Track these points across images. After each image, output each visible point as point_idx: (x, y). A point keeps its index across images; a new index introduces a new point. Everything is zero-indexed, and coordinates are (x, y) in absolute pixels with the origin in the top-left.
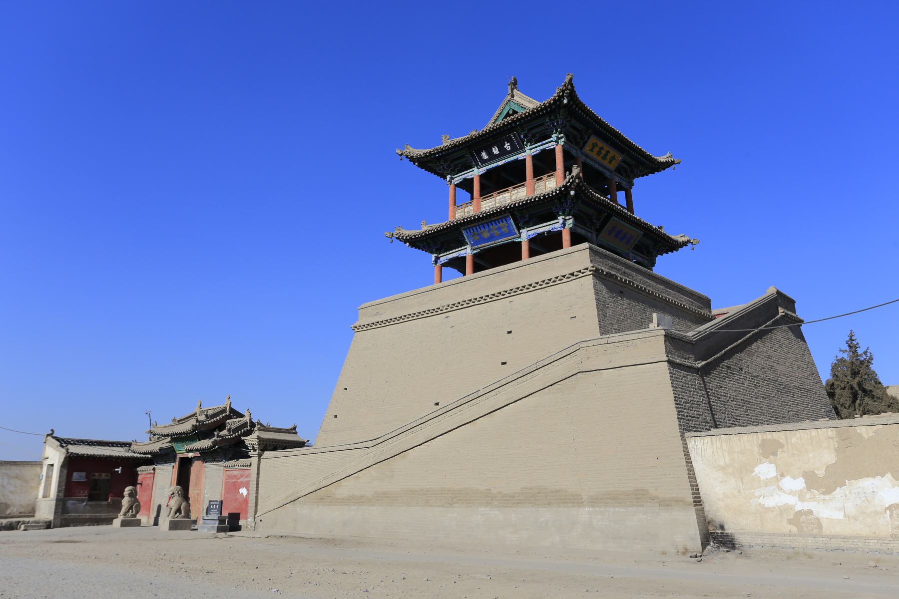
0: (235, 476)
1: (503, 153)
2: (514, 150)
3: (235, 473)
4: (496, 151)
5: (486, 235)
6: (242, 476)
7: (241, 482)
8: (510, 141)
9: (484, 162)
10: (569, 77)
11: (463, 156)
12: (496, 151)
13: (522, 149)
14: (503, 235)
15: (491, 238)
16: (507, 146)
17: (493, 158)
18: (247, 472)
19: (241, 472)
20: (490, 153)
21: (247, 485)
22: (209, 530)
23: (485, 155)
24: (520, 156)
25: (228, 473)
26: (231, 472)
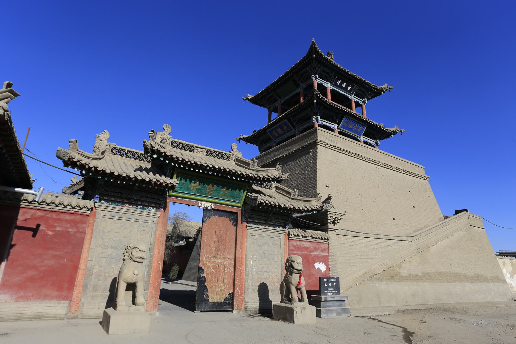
0: (307, 248)
1: (345, 89)
2: (350, 92)
3: (307, 245)
4: (344, 85)
5: (351, 127)
6: (316, 249)
7: (317, 256)
8: (352, 87)
9: (335, 85)
10: (392, 87)
11: (328, 73)
12: (344, 85)
13: (351, 94)
14: (355, 132)
15: (351, 130)
16: (349, 88)
17: (340, 87)
18: (323, 246)
19: (315, 245)
20: (341, 84)
21: (326, 260)
22: (339, 314)
23: (338, 83)
24: (350, 97)
25: (294, 243)
26: (298, 243)
